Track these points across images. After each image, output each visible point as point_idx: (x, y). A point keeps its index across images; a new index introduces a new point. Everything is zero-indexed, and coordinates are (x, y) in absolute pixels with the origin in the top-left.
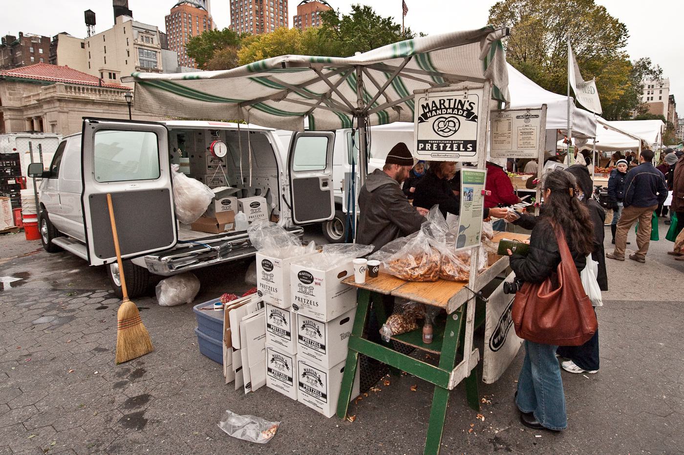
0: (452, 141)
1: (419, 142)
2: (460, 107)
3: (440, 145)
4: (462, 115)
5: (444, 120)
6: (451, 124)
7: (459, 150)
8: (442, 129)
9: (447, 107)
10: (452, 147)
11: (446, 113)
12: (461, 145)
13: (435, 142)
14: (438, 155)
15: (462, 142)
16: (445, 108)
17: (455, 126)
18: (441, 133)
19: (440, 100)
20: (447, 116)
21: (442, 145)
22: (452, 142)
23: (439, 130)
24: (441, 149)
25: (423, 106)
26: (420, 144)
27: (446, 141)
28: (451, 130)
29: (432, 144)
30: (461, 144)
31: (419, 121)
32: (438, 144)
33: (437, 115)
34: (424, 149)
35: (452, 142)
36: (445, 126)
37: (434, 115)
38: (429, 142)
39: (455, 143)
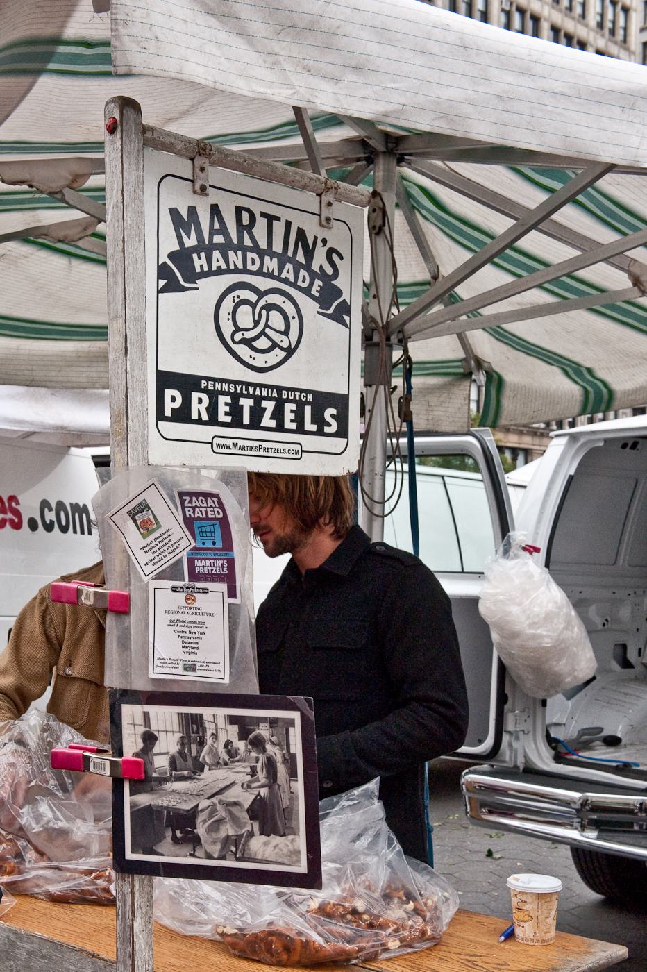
0: (280, 389)
1: (165, 380)
2: (301, 257)
3: (242, 401)
4: (306, 291)
5: (253, 297)
6: (276, 320)
7: (300, 430)
8: (249, 335)
9: (263, 244)
10: (278, 414)
11: (259, 273)
12: (308, 410)
13: (225, 387)
14: (235, 446)
15: (310, 397)
16: (255, 248)
17: (286, 332)
18: (242, 350)
19: (239, 210)
20: (263, 283)
21: (247, 403)
22: (280, 394)
23: (238, 337)
24: (246, 421)
25: (174, 213)
26: (168, 393)
27: (262, 386)
28: (275, 345)
29: (214, 396)
30: (307, 403)
31: (162, 283)
32: (236, 397)
33: (228, 271)
34: (182, 415)
35: (280, 394)
36: (257, 323)
37: (220, 271)
38: (204, 384)
39: (288, 400)
